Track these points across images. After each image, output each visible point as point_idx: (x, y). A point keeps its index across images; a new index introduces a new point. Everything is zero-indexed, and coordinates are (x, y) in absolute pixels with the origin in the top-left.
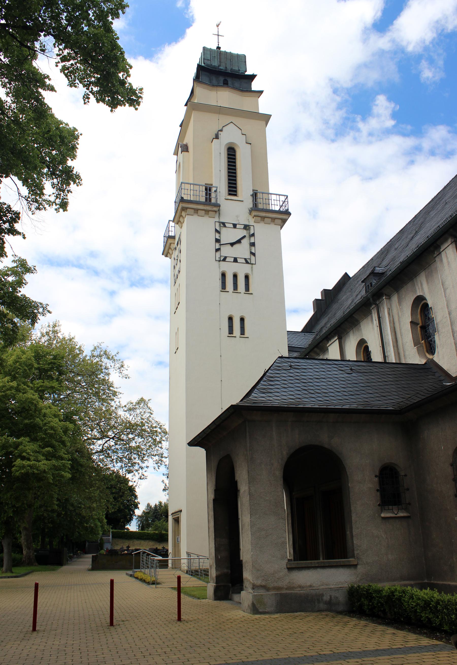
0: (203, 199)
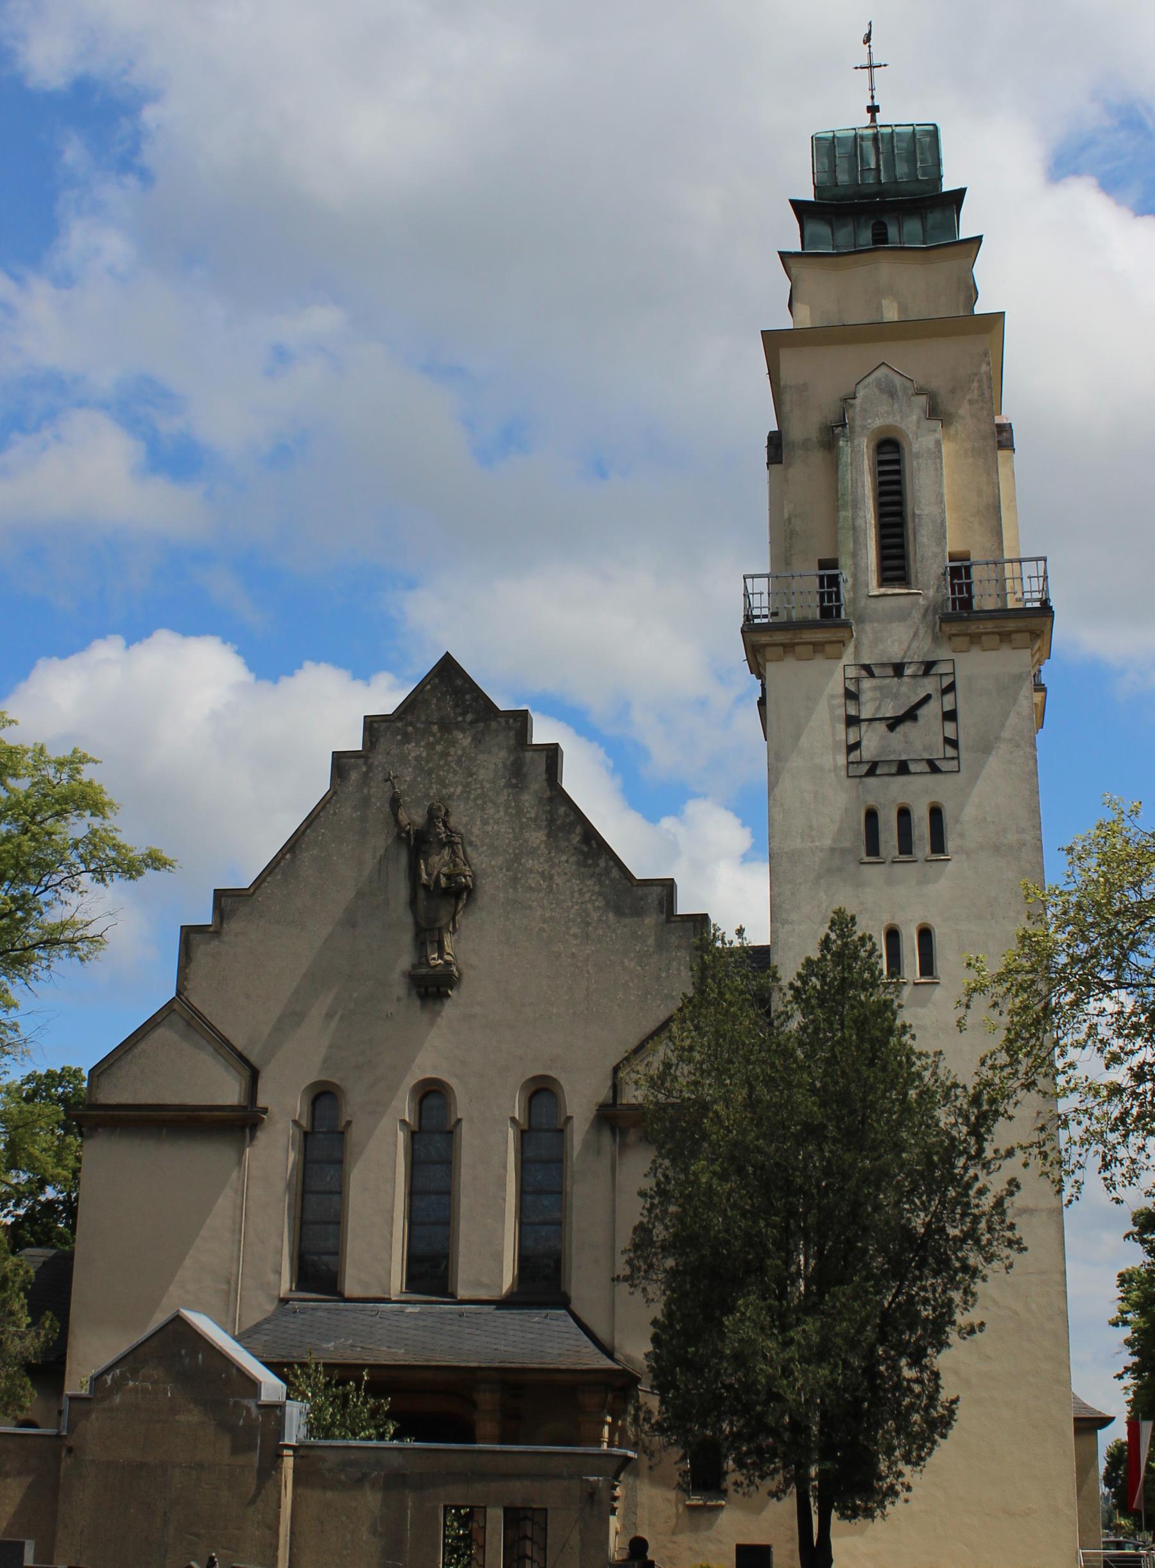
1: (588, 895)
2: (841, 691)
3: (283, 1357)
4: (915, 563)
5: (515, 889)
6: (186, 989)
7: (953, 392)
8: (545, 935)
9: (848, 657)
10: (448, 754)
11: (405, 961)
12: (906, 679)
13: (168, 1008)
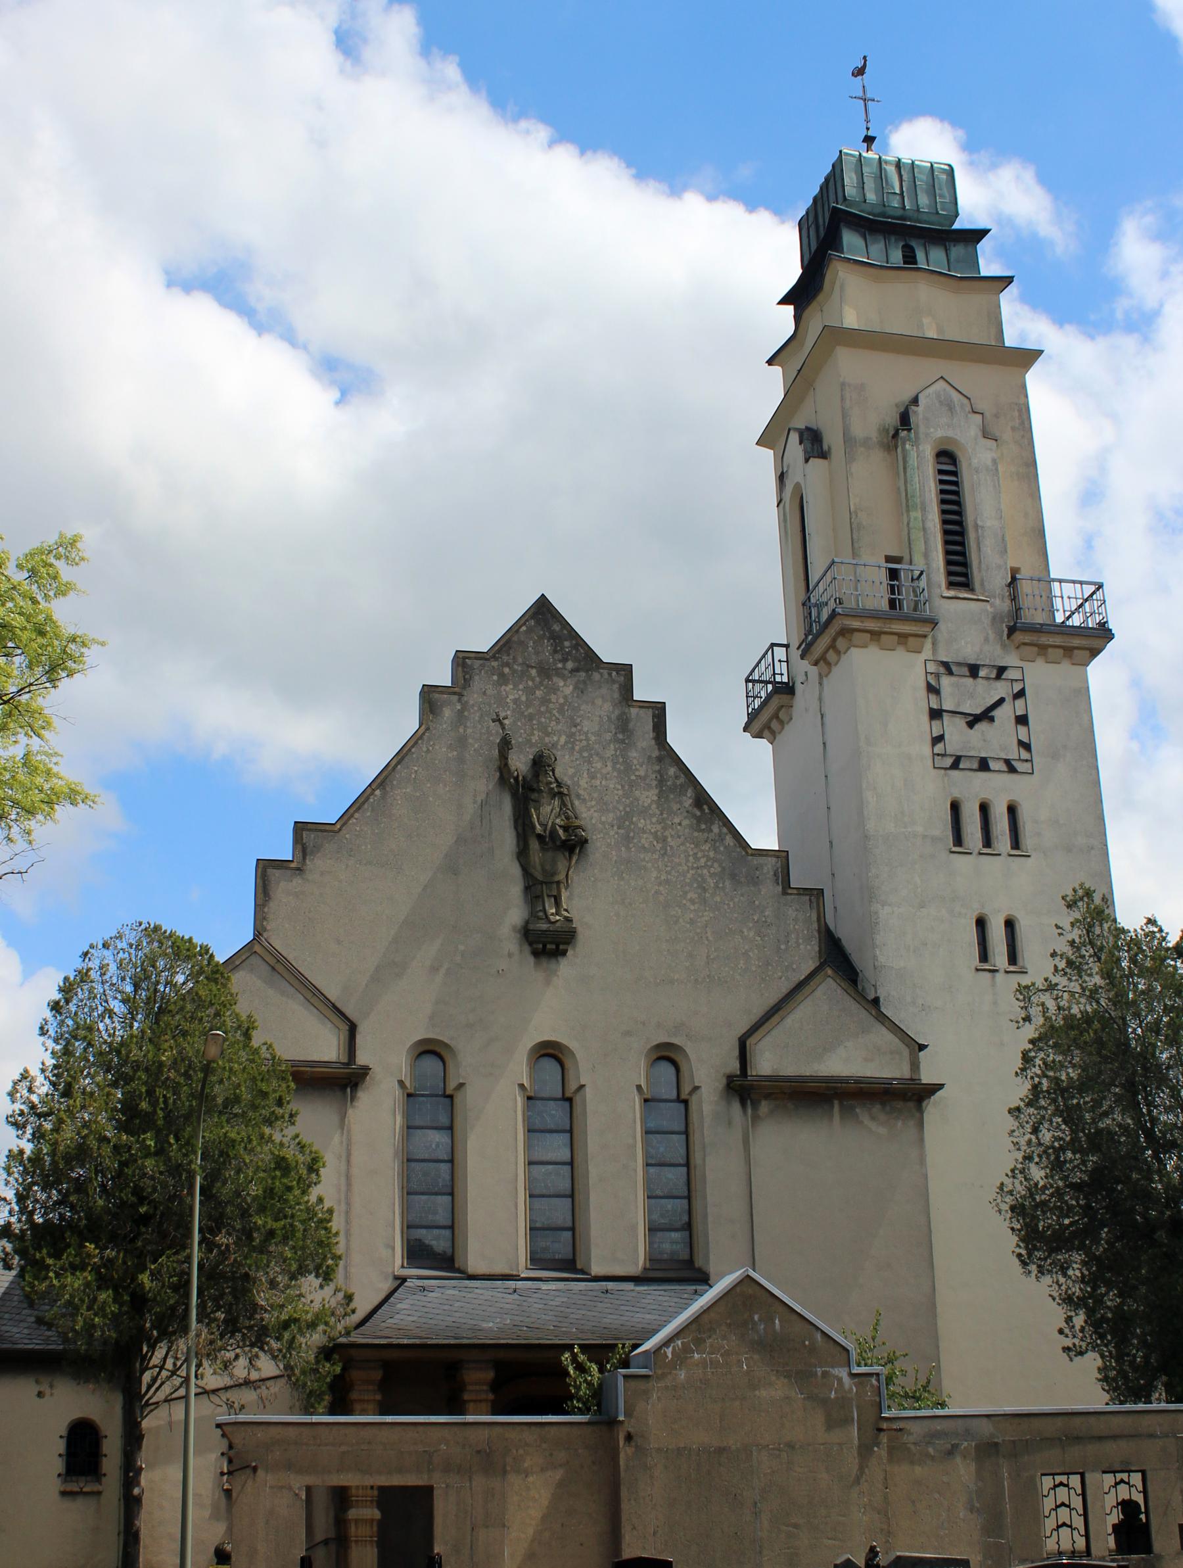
0: (885, 605)
1: (703, 861)
2: (923, 685)
3: (420, 1338)
4: (980, 571)
5: (628, 848)
6: (265, 930)
7: (997, 416)
8: (661, 898)
9: (927, 653)
10: (549, 701)
11: (516, 914)
12: (979, 680)
13: (248, 950)
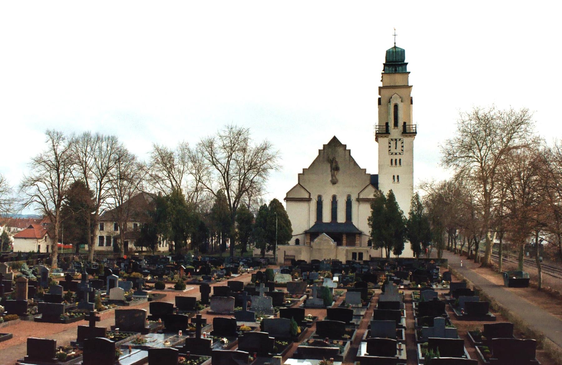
11: (330, 179)
13: (297, 185)
